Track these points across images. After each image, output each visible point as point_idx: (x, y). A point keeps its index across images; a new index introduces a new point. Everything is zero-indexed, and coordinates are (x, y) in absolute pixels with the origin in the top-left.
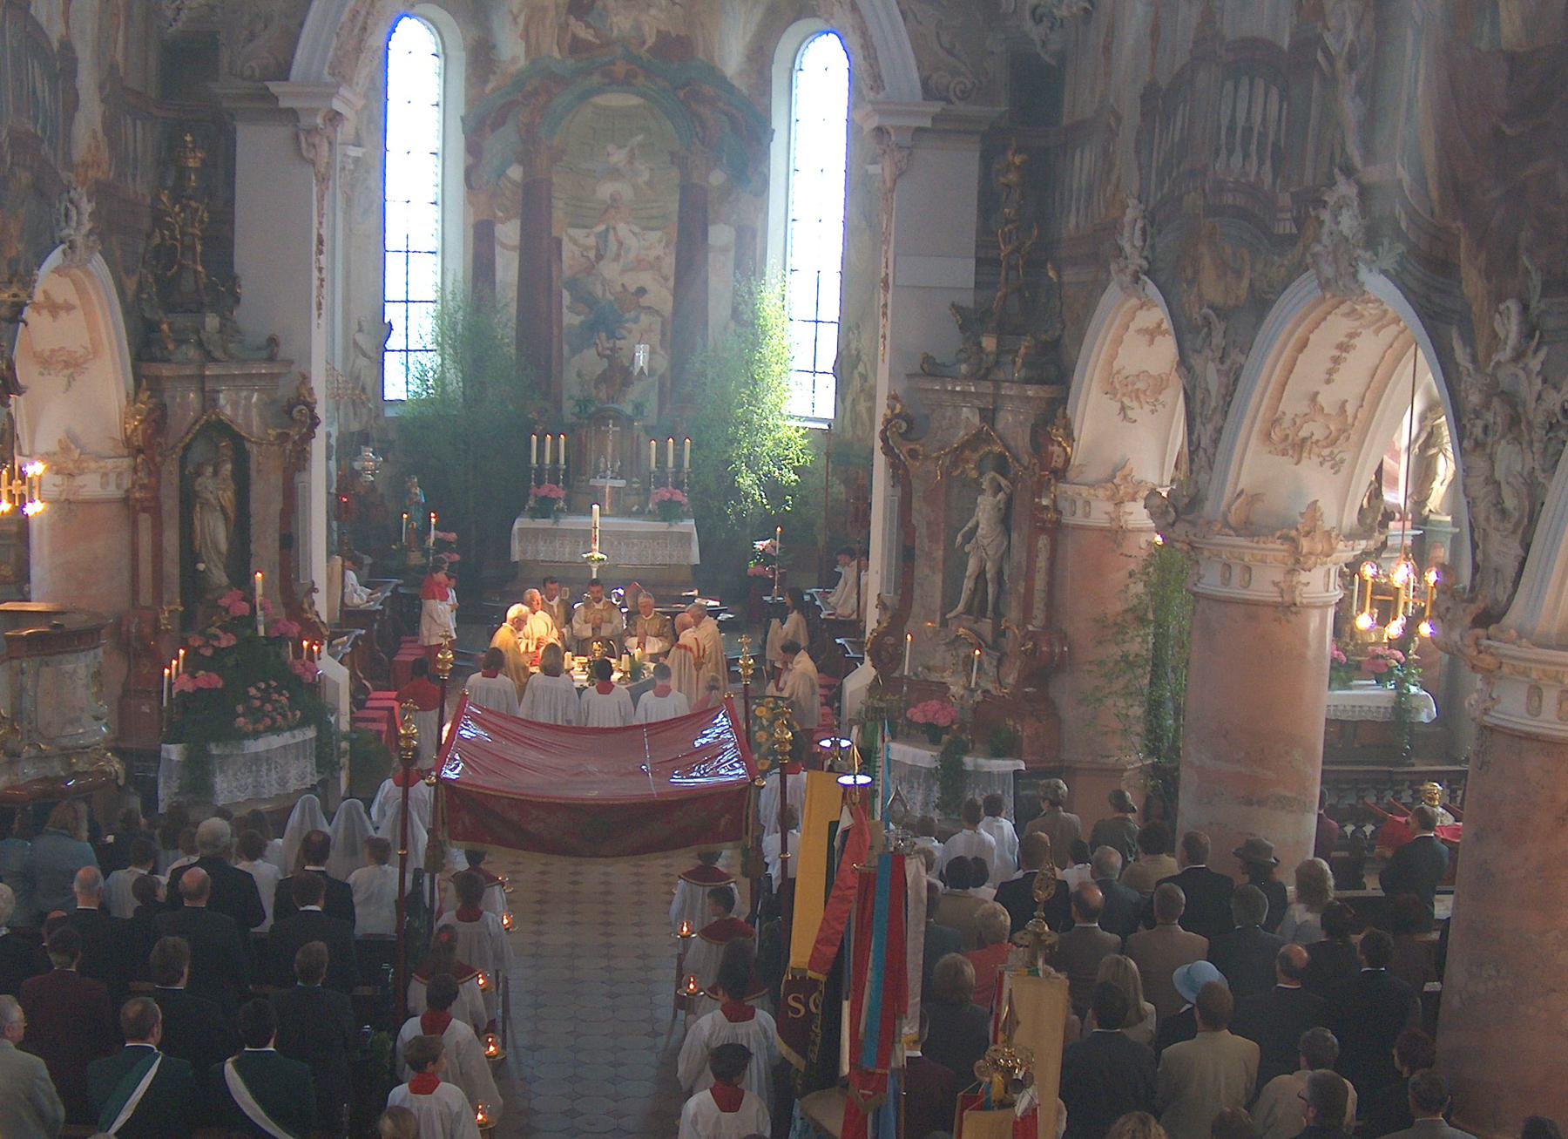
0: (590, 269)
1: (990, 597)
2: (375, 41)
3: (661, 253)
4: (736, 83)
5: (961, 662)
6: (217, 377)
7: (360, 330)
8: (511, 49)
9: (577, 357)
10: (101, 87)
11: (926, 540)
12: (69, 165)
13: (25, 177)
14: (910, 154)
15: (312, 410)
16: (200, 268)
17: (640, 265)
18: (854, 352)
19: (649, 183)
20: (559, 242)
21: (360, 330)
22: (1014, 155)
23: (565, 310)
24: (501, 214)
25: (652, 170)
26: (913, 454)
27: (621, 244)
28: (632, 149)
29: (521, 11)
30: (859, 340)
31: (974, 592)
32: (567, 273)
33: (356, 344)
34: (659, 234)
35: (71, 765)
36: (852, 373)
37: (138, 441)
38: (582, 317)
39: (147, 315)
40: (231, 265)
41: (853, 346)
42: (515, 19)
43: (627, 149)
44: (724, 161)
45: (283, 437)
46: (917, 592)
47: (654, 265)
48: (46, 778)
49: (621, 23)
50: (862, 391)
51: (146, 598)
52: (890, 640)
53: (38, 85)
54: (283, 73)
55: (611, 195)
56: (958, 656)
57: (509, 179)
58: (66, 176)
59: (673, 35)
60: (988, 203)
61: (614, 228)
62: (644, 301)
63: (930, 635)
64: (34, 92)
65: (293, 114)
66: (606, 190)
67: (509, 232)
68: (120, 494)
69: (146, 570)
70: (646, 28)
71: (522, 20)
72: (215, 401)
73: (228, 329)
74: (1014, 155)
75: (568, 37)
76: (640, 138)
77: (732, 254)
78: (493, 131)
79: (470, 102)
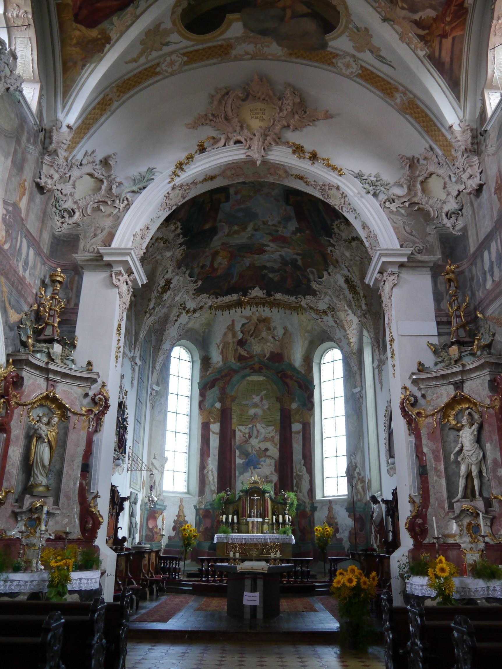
0: (246, 441)
1: (477, 488)
2: (166, 346)
3: (274, 435)
4: (300, 369)
5: (465, 529)
6: (56, 373)
7: (155, 458)
8: (216, 358)
9: (241, 477)
11: (433, 461)
14: (398, 276)
16: (56, 325)
17: (266, 439)
18: (354, 464)
19: (269, 409)
20: (234, 431)
21: (155, 458)
22: (450, 266)
23: (237, 458)
24: (212, 420)
26: (419, 414)
27: (258, 431)
28: (262, 396)
29: (220, 344)
30: (355, 459)
31: (466, 487)
33: (152, 464)
34: (272, 428)
36: (354, 472)
39: (24, 339)
40: (75, 332)
41: (353, 461)
42: (218, 346)
45: (90, 411)
46: (432, 492)
47: (271, 440)
49: (257, 348)
50: (359, 479)
52: (419, 521)
55: (254, 414)
56: (462, 525)
59: (276, 352)
60: (438, 298)
61: (256, 426)
62: (268, 454)
63: (443, 516)
65: (109, 265)
66: (252, 412)
67: (215, 427)
70: (266, 350)
71: (220, 347)
74: (450, 266)
75: (238, 355)
76: (265, 392)
77: (301, 434)
79: (201, 378)
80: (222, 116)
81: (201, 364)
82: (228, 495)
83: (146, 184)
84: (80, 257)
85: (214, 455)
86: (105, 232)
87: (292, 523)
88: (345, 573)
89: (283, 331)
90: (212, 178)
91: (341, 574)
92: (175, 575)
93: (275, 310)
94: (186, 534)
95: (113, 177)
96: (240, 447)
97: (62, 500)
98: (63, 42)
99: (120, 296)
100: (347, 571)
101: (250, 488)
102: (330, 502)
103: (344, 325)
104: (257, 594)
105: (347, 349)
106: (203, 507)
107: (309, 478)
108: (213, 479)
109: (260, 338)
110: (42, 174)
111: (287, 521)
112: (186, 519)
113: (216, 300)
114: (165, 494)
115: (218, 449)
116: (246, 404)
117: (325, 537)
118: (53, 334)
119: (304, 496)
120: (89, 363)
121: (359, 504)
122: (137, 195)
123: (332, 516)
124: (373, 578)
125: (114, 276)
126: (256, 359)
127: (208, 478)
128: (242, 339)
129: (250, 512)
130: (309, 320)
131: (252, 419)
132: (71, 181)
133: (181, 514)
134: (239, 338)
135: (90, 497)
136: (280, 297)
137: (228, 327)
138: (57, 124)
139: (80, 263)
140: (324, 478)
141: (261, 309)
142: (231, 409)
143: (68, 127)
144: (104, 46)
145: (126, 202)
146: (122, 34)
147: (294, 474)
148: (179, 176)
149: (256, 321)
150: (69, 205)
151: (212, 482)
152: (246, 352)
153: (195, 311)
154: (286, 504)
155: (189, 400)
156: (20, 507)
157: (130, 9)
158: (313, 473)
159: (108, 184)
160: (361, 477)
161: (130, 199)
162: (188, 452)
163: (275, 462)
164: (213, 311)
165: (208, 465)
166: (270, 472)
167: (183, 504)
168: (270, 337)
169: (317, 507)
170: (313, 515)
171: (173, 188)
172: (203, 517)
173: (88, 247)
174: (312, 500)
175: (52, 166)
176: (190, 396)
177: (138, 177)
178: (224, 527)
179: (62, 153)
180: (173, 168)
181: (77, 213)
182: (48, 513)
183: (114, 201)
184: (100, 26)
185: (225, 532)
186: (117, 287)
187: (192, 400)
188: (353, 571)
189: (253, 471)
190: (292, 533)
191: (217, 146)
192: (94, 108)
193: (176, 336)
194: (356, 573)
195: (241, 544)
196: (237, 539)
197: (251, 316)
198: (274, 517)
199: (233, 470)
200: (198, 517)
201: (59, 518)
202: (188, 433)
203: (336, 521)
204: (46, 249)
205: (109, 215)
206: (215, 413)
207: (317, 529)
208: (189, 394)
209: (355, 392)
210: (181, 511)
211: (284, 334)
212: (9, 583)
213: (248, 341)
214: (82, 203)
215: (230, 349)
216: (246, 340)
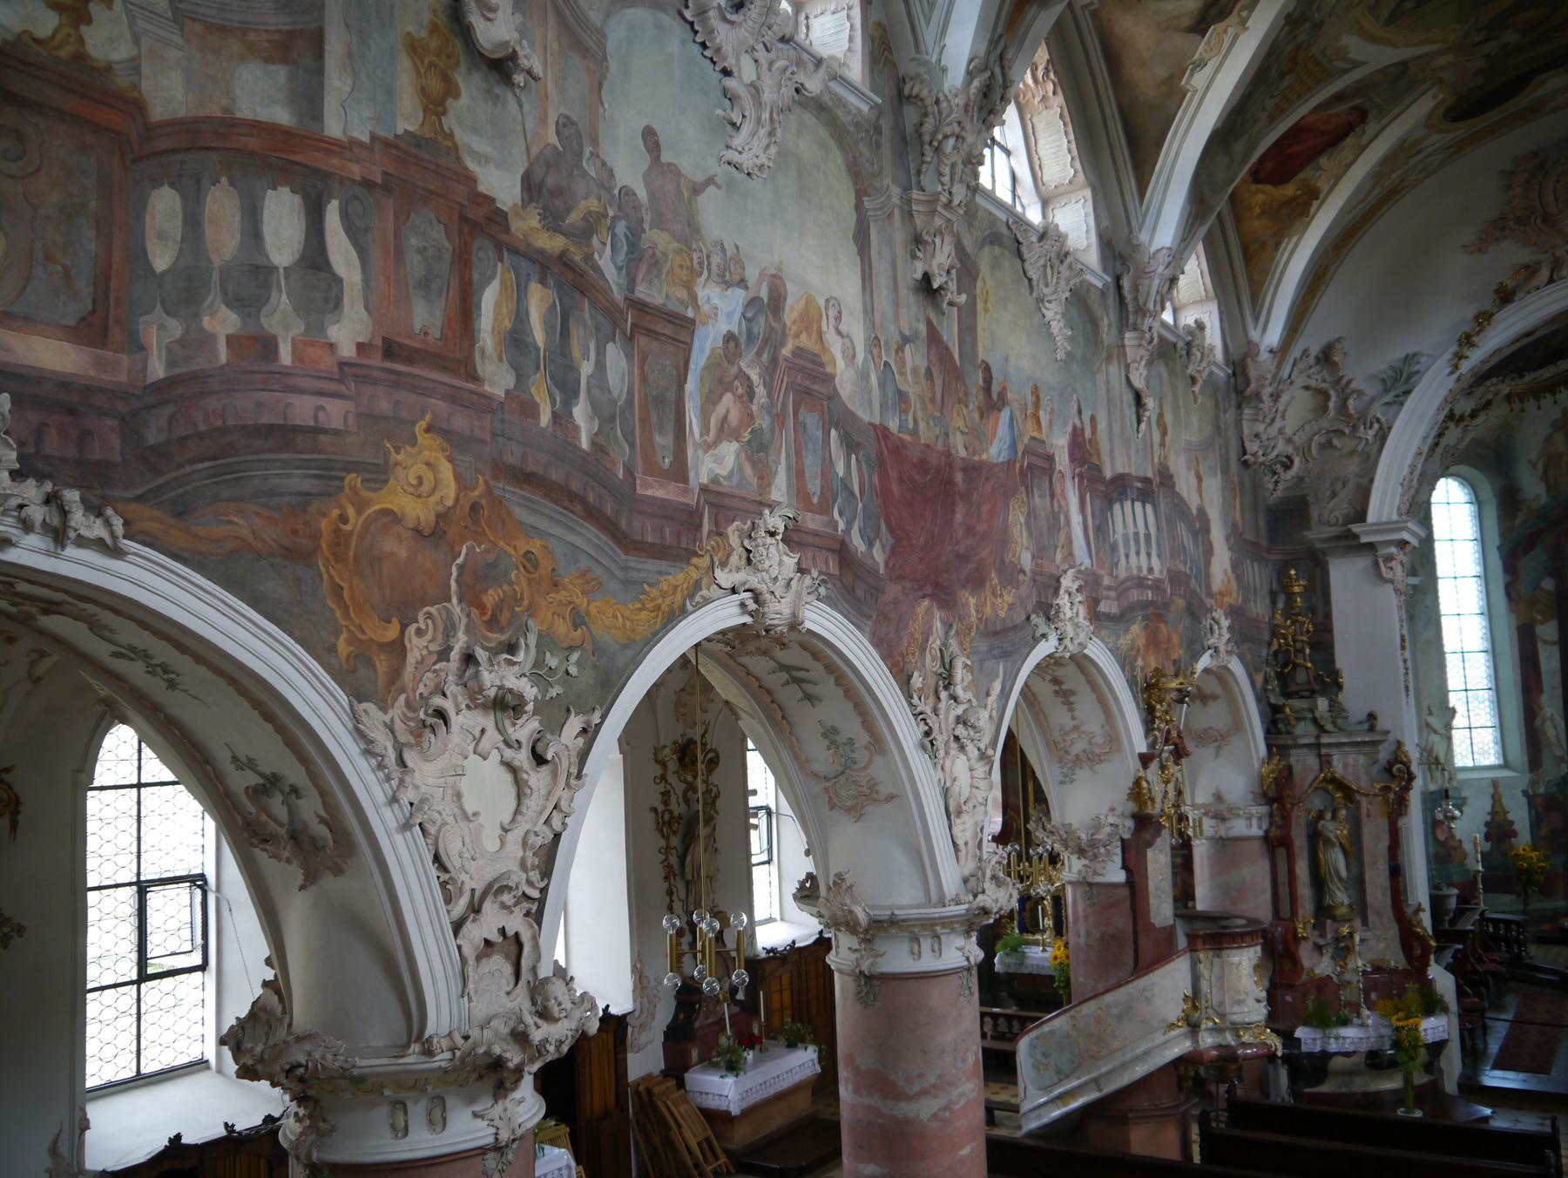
7: (1430, 713)
8: (1533, 488)
10: (1228, 539)
12: (1210, 594)
13: (1180, 603)
15: (1408, 768)
16: (1309, 665)
24: (1539, 618)
33: (1428, 725)
35: (1239, 1036)
37: (1272, 793)
39: (1273, 701)
40: (1333, 661)
45: (1386, 789)
48: (1220, 1046)
51: (1285, 911)
53: (1185, 539)
54: (1361, 516)
58: (1209, 602)
64: (1184, 547)
65: (1371, 546)
68: (1260, 833)
69: (1284, 891)
71: (1540, 466)
72: (1329, 763)
73: (1336, 709)
79: (1503, 534)
80: (1539, 221)
83: (1406, 387)
84: (1317, 534)
85: (1554, 688)
86: (1351, 486)
90: (1528, 334)
95: (1344, 381)
97: (1372, 918)
98: (1238, 219)
99: (1396, 590)
106: (1541, 790)
108: (1557, 736)
110: (1245, 439)
112: (1510, 817)
114: (1460, 776)
118: (1309, 682)
120: (1371, 717)
122: (1394, 408)
125: (1382, 564)
132: (1279, 414)
133: (1499, 809)
135: (1409, 911)
138: (1251, 349)
139: (1319, 545)
143: (1271, 351)
144: (1308, 204)
145: (1376, 426)
146: (1338, 178)
148: (1467, 358)
150: (1281, 447)
151: (1554, 740)
153: (1474, 414)
156: (1322, 936)
157: (1349, 141)
159: (1338, 396)
161: (1383, 420)
164: (1517, 406)
167: (1501, 789)
171: (1458, 379)
173: (1326, 516)
175: (1256, 420)
177: (1390, 373)
179: (1267, 391)
180: (1454, 348)
181: (1297, 461)
182: (1362, 941)
183: (1355, 428)
184: (1299, 177)
186: (1391, 581)
191: (1535, 283)
192: (1304, 297)
200: (1533, 812)
201: (1372, 943)
204: (1264, 542)
205: (1353, 452)
212: (1341, 1041)
214: (1300, 439)
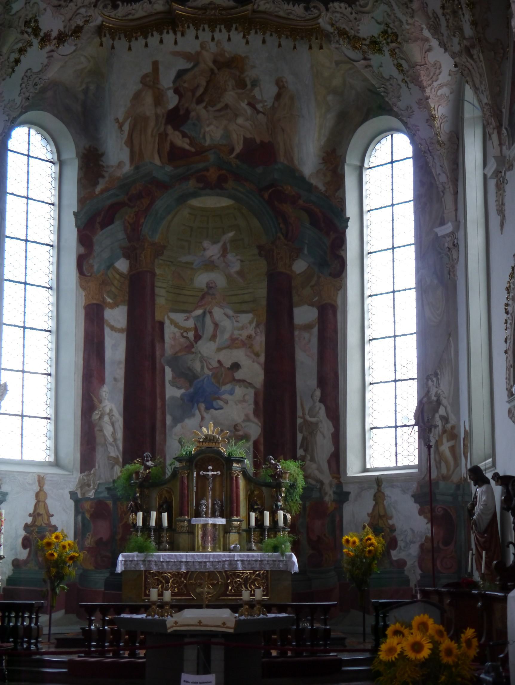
0: (189, 348)
3: (253, 333)
4: (314, 181)
9: (179, 426)
18: (434, 398)
19: (240, 273)
20: (162, 324)
23: (167, 385)
24: (109, 300)
25: (242, 261)
27: (216, 325)
28: (225, 244)
30: (438, 386)
32: (169, 351)
34: (250, 316)
36: (433, 416)
38: (183, 391)
41: (433, 391)
42: (121, 127)
43: (220, 244)
44: (306, 252)
50: (444, 431)
55: (208, 284)
57: (117, 271)
59: (258, 141)
61: (210, 313)
62: (239, 375)
70: (235, 136)
71: (126, 128)
75: (167, 147)
76: (231, 234)
77: (315, 330)
78: (103, 227)
79: (81, 201)
81: (80, 169)
82: (147, 467)
85: (115, 380)
87: (293, 528)
88: (406, 631)
89: (275, 90)
91: (397, 633)
92: (29, 643)
93: (255, 38)
94: (52, 555)
96: (174, 362)
100: (409, 626)
101: (198, 453)
102: (378, 480)
103: (419, 76)
104: (211, 678)
105: (424, 132)
106: (91, 494)
107: (332, 430)
108: (114, 433)
109: (219, 106)
111: (281, 523)
112: (54, 521)
113: (112, 14)
115: (123, 366)
116: (187, 263)
117: (365, 557)
119: (319, 469)
121: (442, 485)
123: (382, 513)
124: (469, 643)
126: (212, 157)
127: (101, 430)
128: (176, 109)
129: (198, 505)
130: (337, 63)
131: (203, 297)
133: (41, 511)
134: (171, 106)
136: (268, 6)
137: (144, 80)
140: (367, 427)
141: (221, 35)
142: (154, 275)
147: (299, 421)
149: (211, 65)
151: (110, 439)
152: (188, 141)
153: (61, 38)
154: (279, 486)
155: (53, 252)
158: (341, 418)
160: (449, 426)
162: (53, 373)
163: (256, 395)
164: (107, 40)
165: (100, 402)
166: (243, 417)
167: (46, 488)
168: (244, 105)
169: (349, 493)
170: (339, 509)
172: (92, 516)
174: (338, 478)
176: (55, 244)
178: (139, 538)
185: (141, 549)
187: (62, 253)
188: (423, 626)
189: (205, 415)
190: (293, 550)
193: (18, 100)
194: (431, 631)
195: (178, 575)
196: (168, 562)
197: (198, 54)
198: (253, 515)
199: (159, 412)
200: (80, 518)
202: (54, 329)
203: (391, 522)
206: (116, 282)
207: (348, 541)
208: (52, 238)
209: (440, 234)
210: (41, 504)
211: (278, 97)
213: (193, 114)
215: (149, 131)
216: (188, 112)
